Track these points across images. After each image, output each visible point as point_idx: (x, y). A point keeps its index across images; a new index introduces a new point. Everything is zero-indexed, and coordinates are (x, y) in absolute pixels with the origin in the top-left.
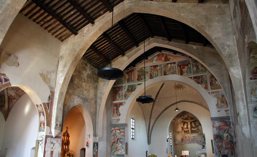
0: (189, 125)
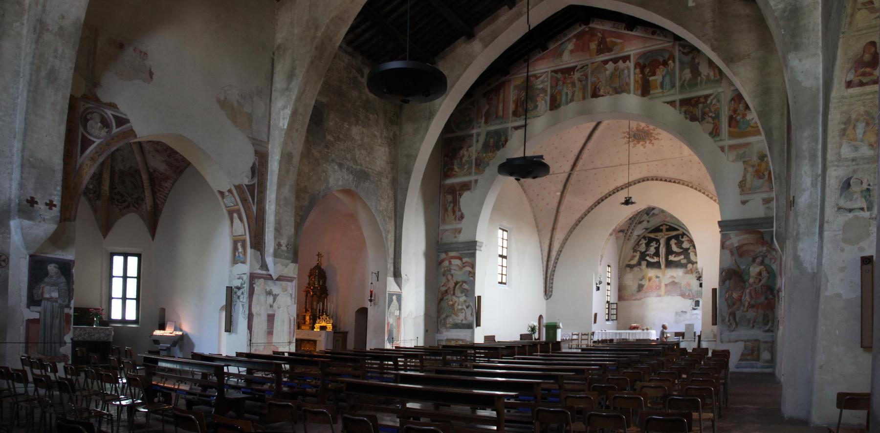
0: (661, 246)
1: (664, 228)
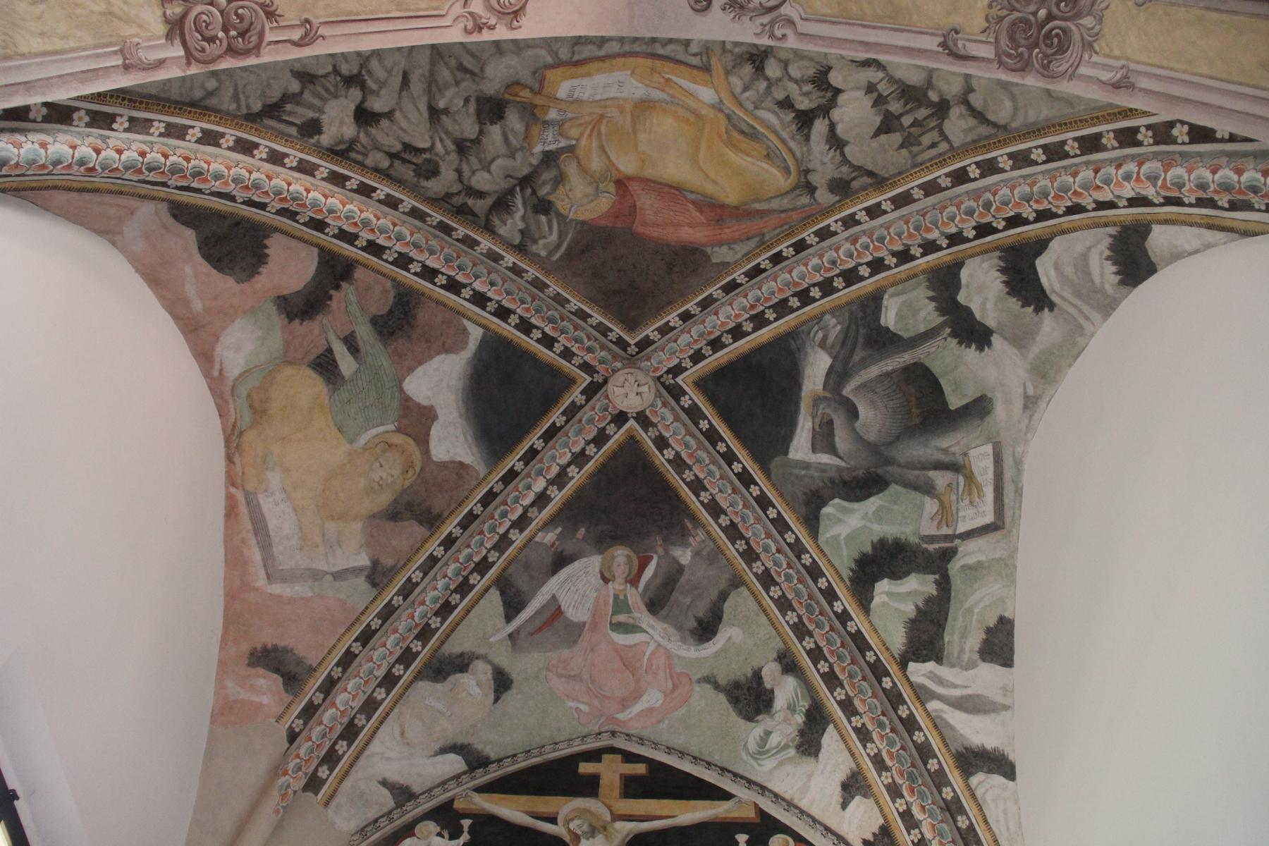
1: (610, 772)
